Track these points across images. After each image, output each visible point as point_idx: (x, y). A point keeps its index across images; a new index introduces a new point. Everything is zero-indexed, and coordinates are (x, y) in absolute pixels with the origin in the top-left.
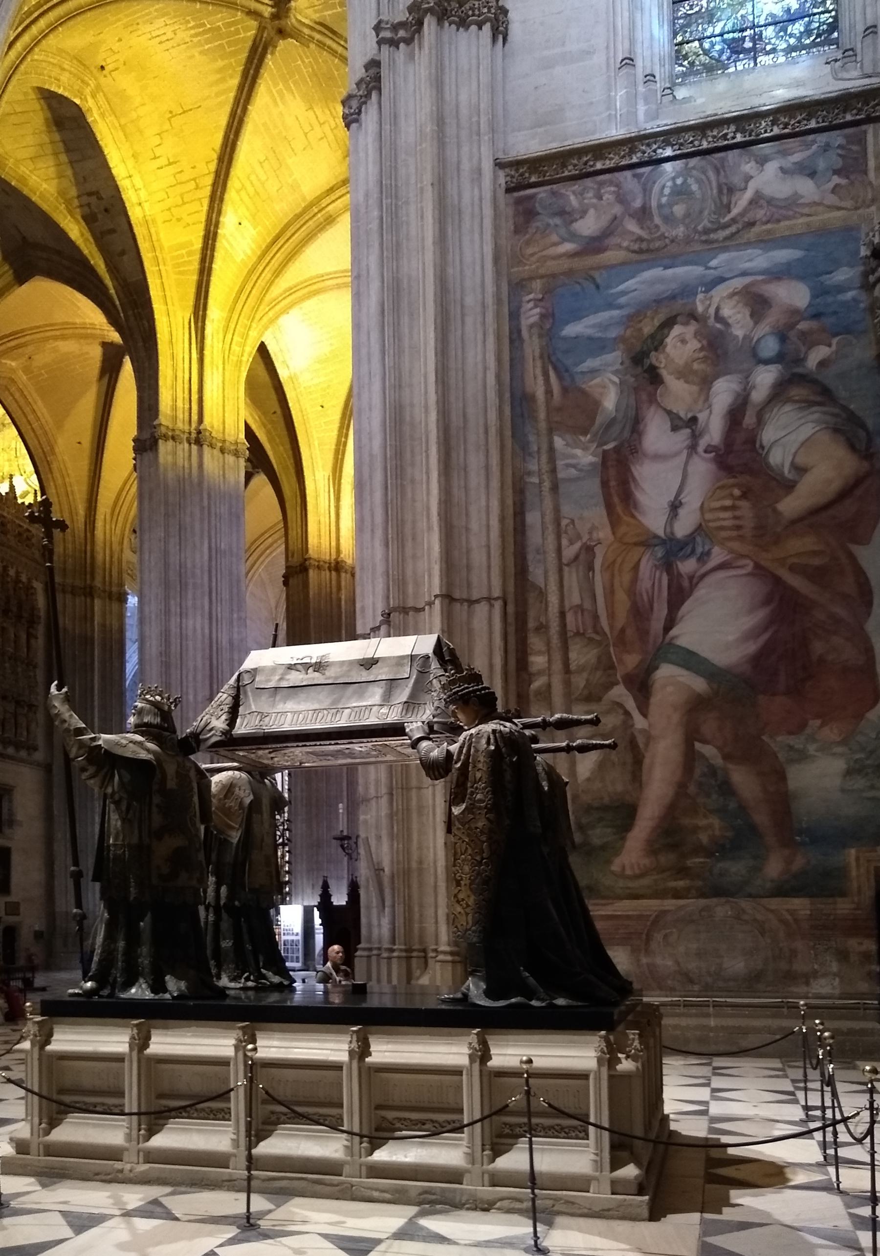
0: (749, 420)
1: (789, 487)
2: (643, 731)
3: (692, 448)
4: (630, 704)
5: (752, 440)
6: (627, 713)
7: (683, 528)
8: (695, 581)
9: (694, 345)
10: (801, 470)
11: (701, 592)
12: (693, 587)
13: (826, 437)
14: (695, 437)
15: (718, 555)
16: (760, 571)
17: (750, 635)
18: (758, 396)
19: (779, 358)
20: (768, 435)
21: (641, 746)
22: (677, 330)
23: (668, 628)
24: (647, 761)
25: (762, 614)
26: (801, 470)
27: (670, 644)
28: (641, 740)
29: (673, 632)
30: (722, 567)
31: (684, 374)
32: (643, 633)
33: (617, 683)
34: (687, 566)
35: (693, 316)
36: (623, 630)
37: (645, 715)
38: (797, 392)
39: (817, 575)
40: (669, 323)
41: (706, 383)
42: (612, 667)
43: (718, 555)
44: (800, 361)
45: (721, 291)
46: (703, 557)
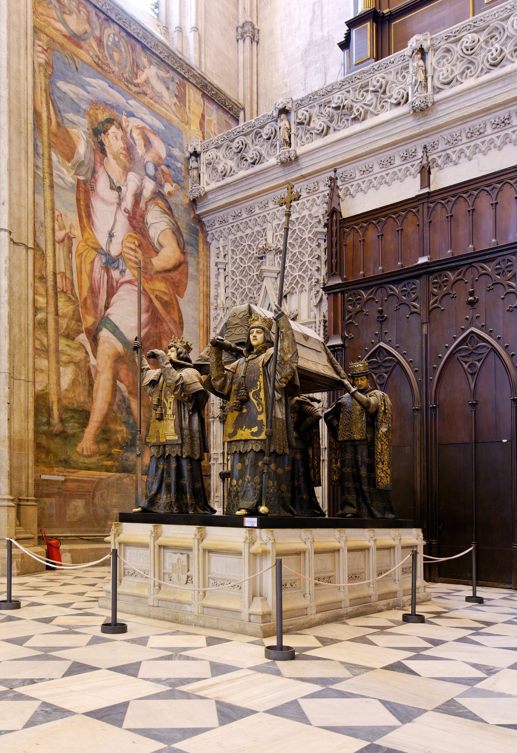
2: (94, 366)
4: (89, 348)
6: (87, 353)
12: (118, 288)
21: (93, 375)
23: (107, 308)
24: (95, 386)
27: (107, 317)
28: (93, 372)
29: (109, 311)
30: (129, 282)
32: (96, 306)
33: (82, 332)
36: (85, 299)
37: (95, 357)
42: (79, 320)
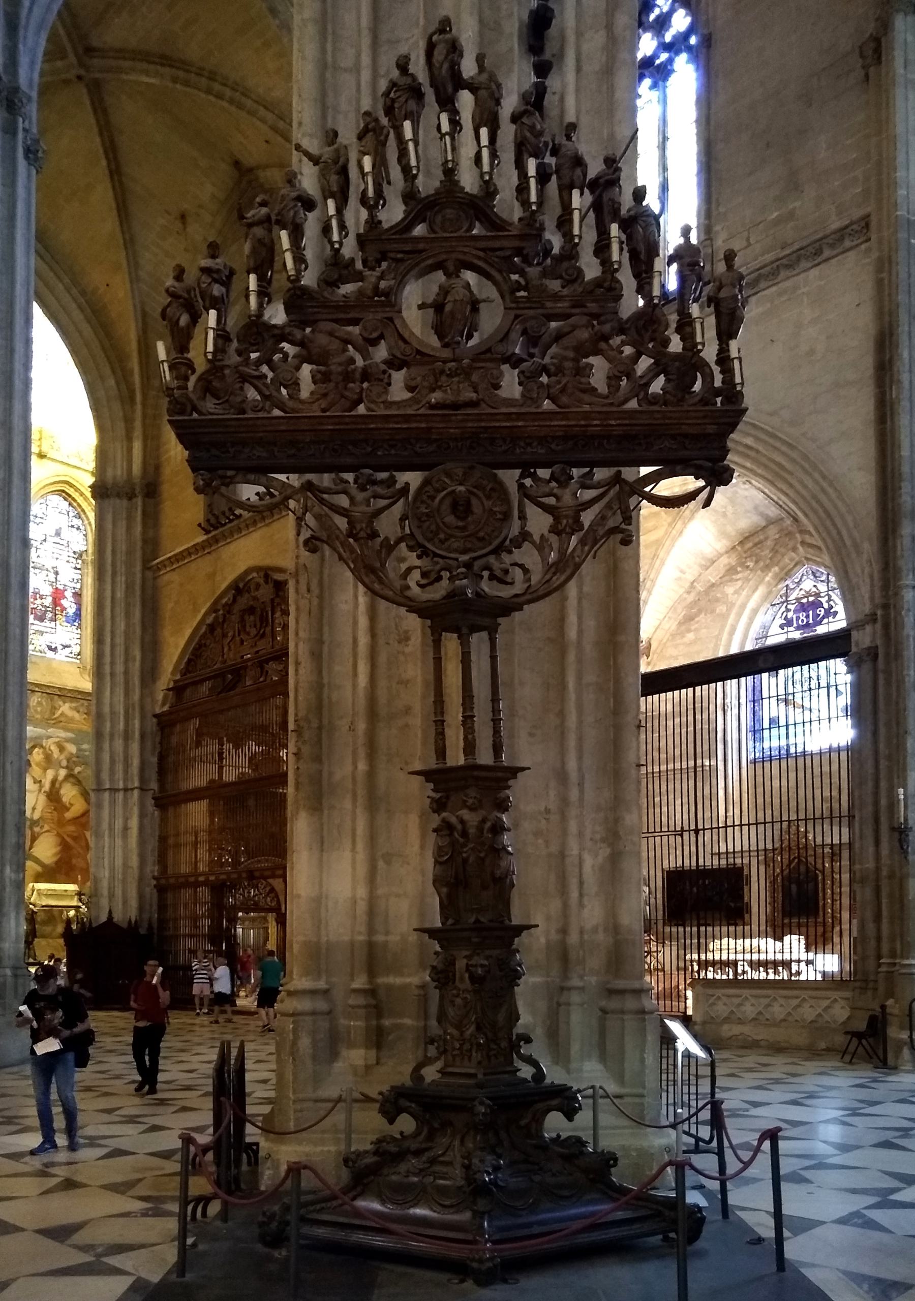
0: (57, 785)
1: (68, 809)
3: (40, 791)
5: (58, 792)
7: (36, 816)
8: (39, 834)
9: (41, 756)
10: (72, 805)
11: (41, 838)
13: (79, 796)
14: (41, 787)
15: (46, 828)
16: (58, 835)
17: (55, 854)
18: (60, 778)
19: (67, 767)
20: (62, 792)
22: (36, 750)
25: (59, 848)
26: (72, 805)
31: (38, 765)
34: (37, 829)
35: (42, 746)
38: (72, 780)
39: (75, 839)
40: (34, 747)
41: (45, 770)
43: (46, 828)
44: (72, 770)
45: (51, 741)
46: (42, 827)
